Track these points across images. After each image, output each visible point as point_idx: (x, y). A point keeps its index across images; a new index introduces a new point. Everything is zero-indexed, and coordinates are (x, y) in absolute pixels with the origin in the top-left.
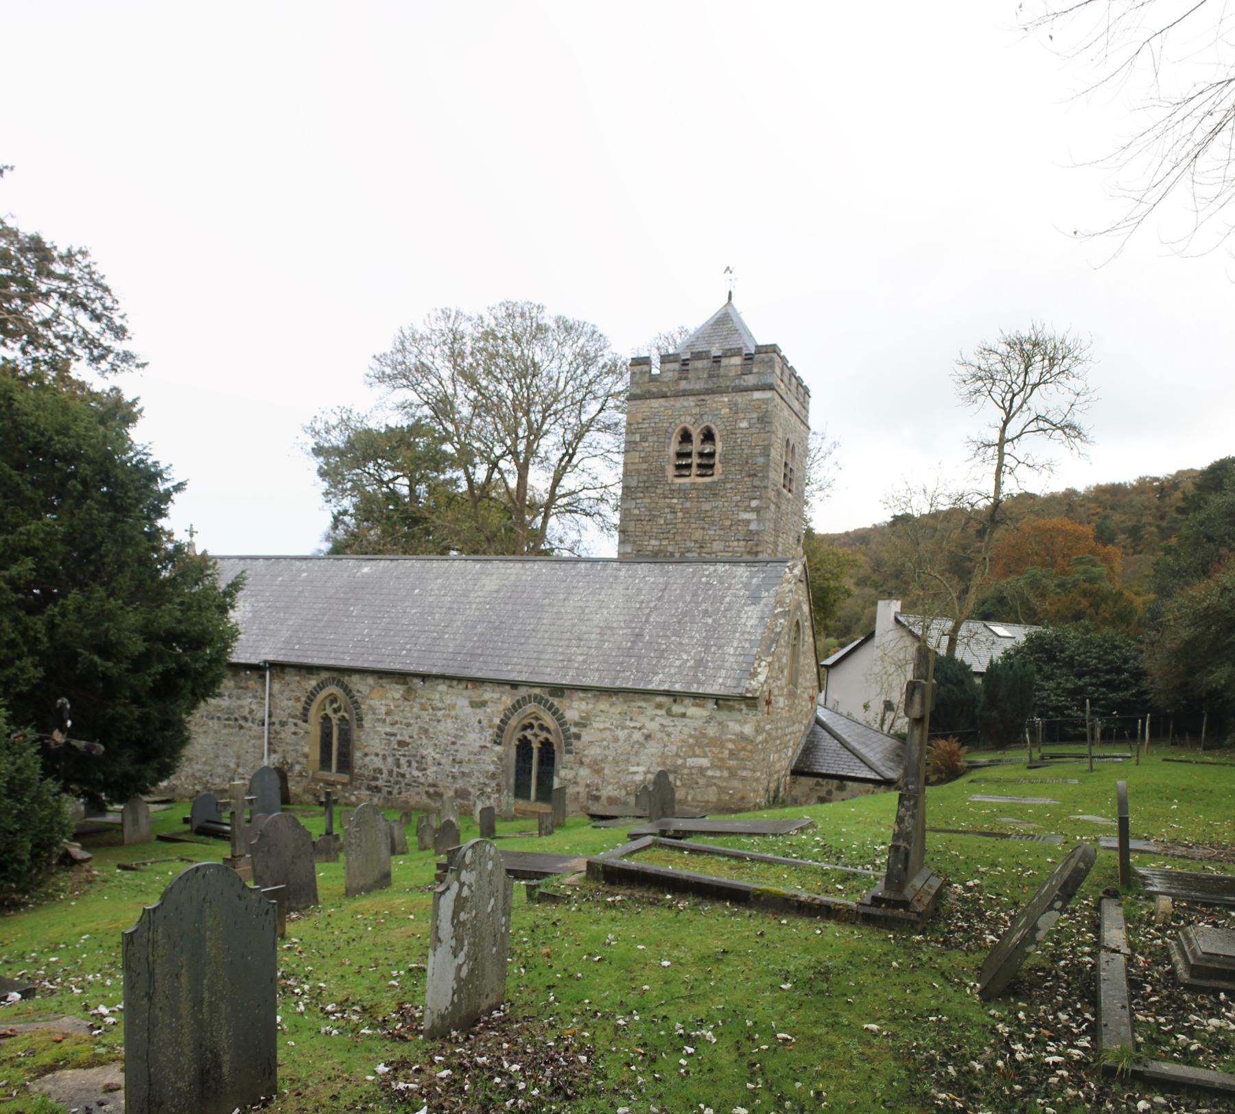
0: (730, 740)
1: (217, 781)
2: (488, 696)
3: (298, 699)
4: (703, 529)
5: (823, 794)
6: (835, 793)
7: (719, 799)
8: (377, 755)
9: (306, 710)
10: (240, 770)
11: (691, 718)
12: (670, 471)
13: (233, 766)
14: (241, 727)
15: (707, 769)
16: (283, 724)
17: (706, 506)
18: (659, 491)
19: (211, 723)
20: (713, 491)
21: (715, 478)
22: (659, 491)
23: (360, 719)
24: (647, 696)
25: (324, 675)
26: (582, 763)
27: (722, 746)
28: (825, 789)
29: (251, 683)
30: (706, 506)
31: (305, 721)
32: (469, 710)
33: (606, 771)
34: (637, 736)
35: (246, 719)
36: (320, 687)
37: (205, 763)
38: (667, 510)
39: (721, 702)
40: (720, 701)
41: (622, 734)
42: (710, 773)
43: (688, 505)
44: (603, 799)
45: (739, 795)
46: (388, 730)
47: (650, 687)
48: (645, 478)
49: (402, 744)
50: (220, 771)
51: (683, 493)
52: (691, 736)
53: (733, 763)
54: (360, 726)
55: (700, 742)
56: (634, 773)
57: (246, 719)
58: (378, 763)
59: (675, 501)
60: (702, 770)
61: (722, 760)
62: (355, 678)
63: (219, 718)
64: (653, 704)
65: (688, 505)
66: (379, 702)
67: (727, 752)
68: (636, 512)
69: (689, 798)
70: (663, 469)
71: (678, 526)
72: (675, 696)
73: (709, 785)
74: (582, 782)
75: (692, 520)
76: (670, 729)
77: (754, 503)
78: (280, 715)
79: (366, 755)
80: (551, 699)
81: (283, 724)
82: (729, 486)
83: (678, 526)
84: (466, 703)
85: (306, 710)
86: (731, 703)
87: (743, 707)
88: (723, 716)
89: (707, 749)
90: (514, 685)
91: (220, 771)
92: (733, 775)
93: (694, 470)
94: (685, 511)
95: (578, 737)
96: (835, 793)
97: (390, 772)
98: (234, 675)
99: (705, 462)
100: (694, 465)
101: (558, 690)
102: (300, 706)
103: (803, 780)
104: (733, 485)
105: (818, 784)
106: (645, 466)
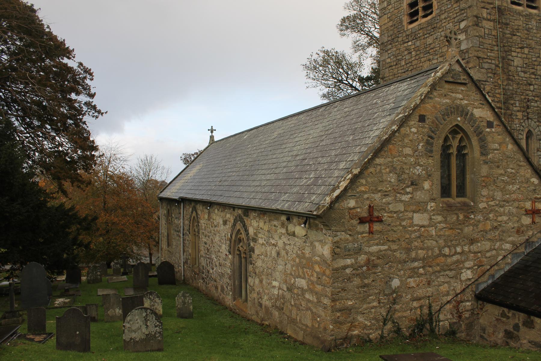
0: (317, 262)
4: (429, 60)
5: (510, 328)
6: (523, 329)
7: (313, 325)
11: (298, 237)
12: (406, 19)
15: (306, 291)
17: (430, 40)
18: (400, 39)
20: (433, 27)
21: (434, 14)
22: (400, 39)
24: (277, 216)
26: (255, 273)
27: (312, 269)
28: (512, 322)
30: (430, 40)
32: (222, 227)
33: (264, 282)
34: (274, 254)
38: (406, 53)
39: (312, 221)
40: (308, 219)
41: (269, 248)
42: (307, 296)
43: (418, 43)
44: (263, 307)
45: (322, 326)
47: (274, 207)
48: (391, 32)
51: (414, 36)
52: (298, 256)
53: (319, 288)
55: (304, 263)
56: (274, 287)
59: (410, 43)
60: (303, 291)
61: (313, 283)
64: (280, 222)
65: (418, 43)
67: (315, 275)
68: (388, 60)
69: (298, 319)
70: (401, 22)
71: (414, 63)
72: (290, 215)
73: (308, 309)
74: (257, 290)
75: (422, 56)
76: (287, 247)
77: (463, 25)
80: (244, 217)
82: (443, 17)
83: (414, 63)
86: (317, 222)
87: (322, 227)
88: (313, 234)
89: (305, 270)
90: (233, 207)
92: (319, 301)
93: (421, 14)
94: (417, 49)
95: (252, 250)
96: (523, 329)
99: (427, 4)
100: (420, 9)
101: (247, 210)
103: (489, 307)
104: (446, 14)
105: (503, 315)
106: (391, 23)
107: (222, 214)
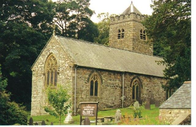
1: (109, 104)
2: (163, 81)
3: (129, 81)
8: (145, 94)
9: (131, 84)
10: (116, 100)
13: (114, 99)
14: (116, 89)
16: (126, 87)
19: (108, 87)
23: (142, 86)
25: (135, 75)
29: (118, 77)
31: (131, 87)
35: (117, 86)
36: (134, 78)
37: (106, 99)
46: (147, 88)
49: (150, 91)
50: (111, 101)
54: (142, 88)
57: (117, 86)
58: (145, 96)
62: (141, 77)
63: (110, 86)
66: (145, 81)
78: (126, 85)
79: (143, 94)
81: (126, 87)
84: (159, 82)
85: (131, 84)
91: (111, 101)
97: (148, 98)
98: (114, 74)
102: (130, 83)
107: (160, 80)
